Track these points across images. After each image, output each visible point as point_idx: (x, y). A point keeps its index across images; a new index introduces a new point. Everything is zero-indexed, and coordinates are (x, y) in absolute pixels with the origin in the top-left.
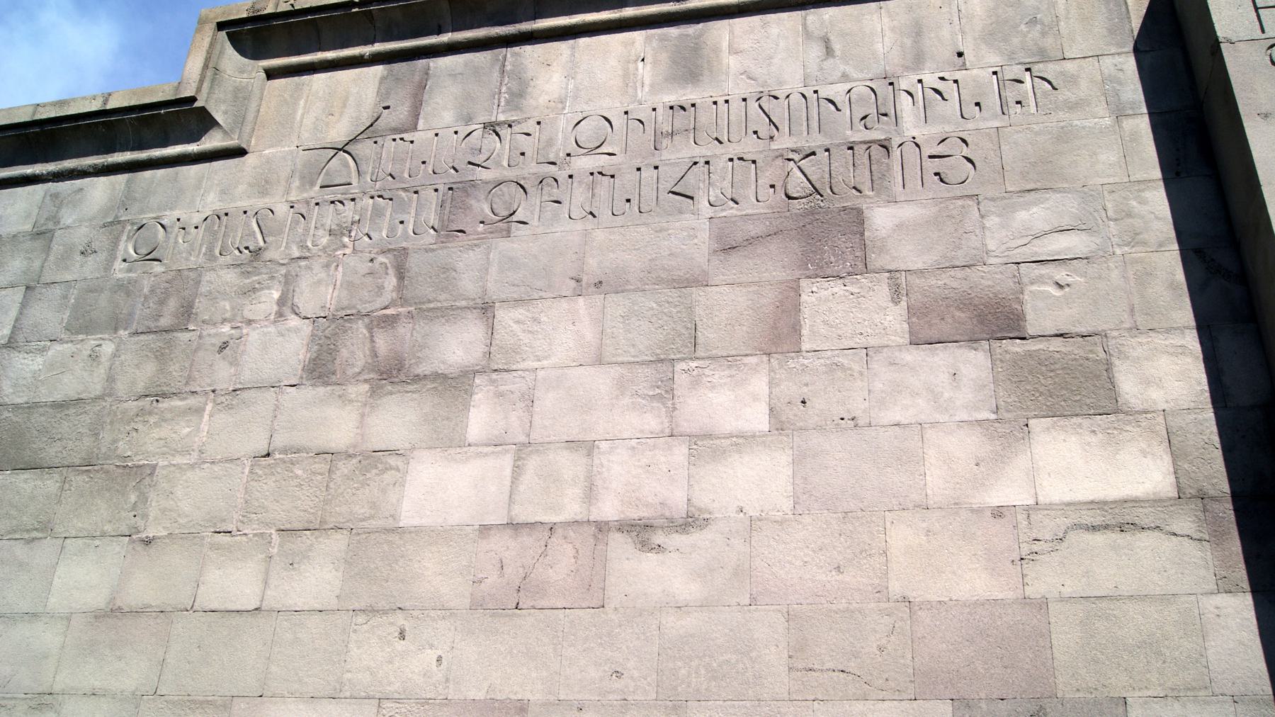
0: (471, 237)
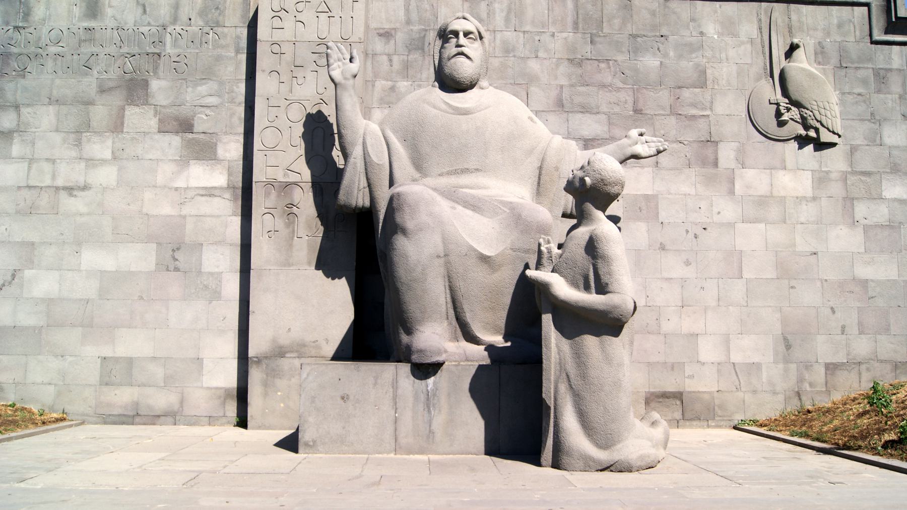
0: (11, 77)
